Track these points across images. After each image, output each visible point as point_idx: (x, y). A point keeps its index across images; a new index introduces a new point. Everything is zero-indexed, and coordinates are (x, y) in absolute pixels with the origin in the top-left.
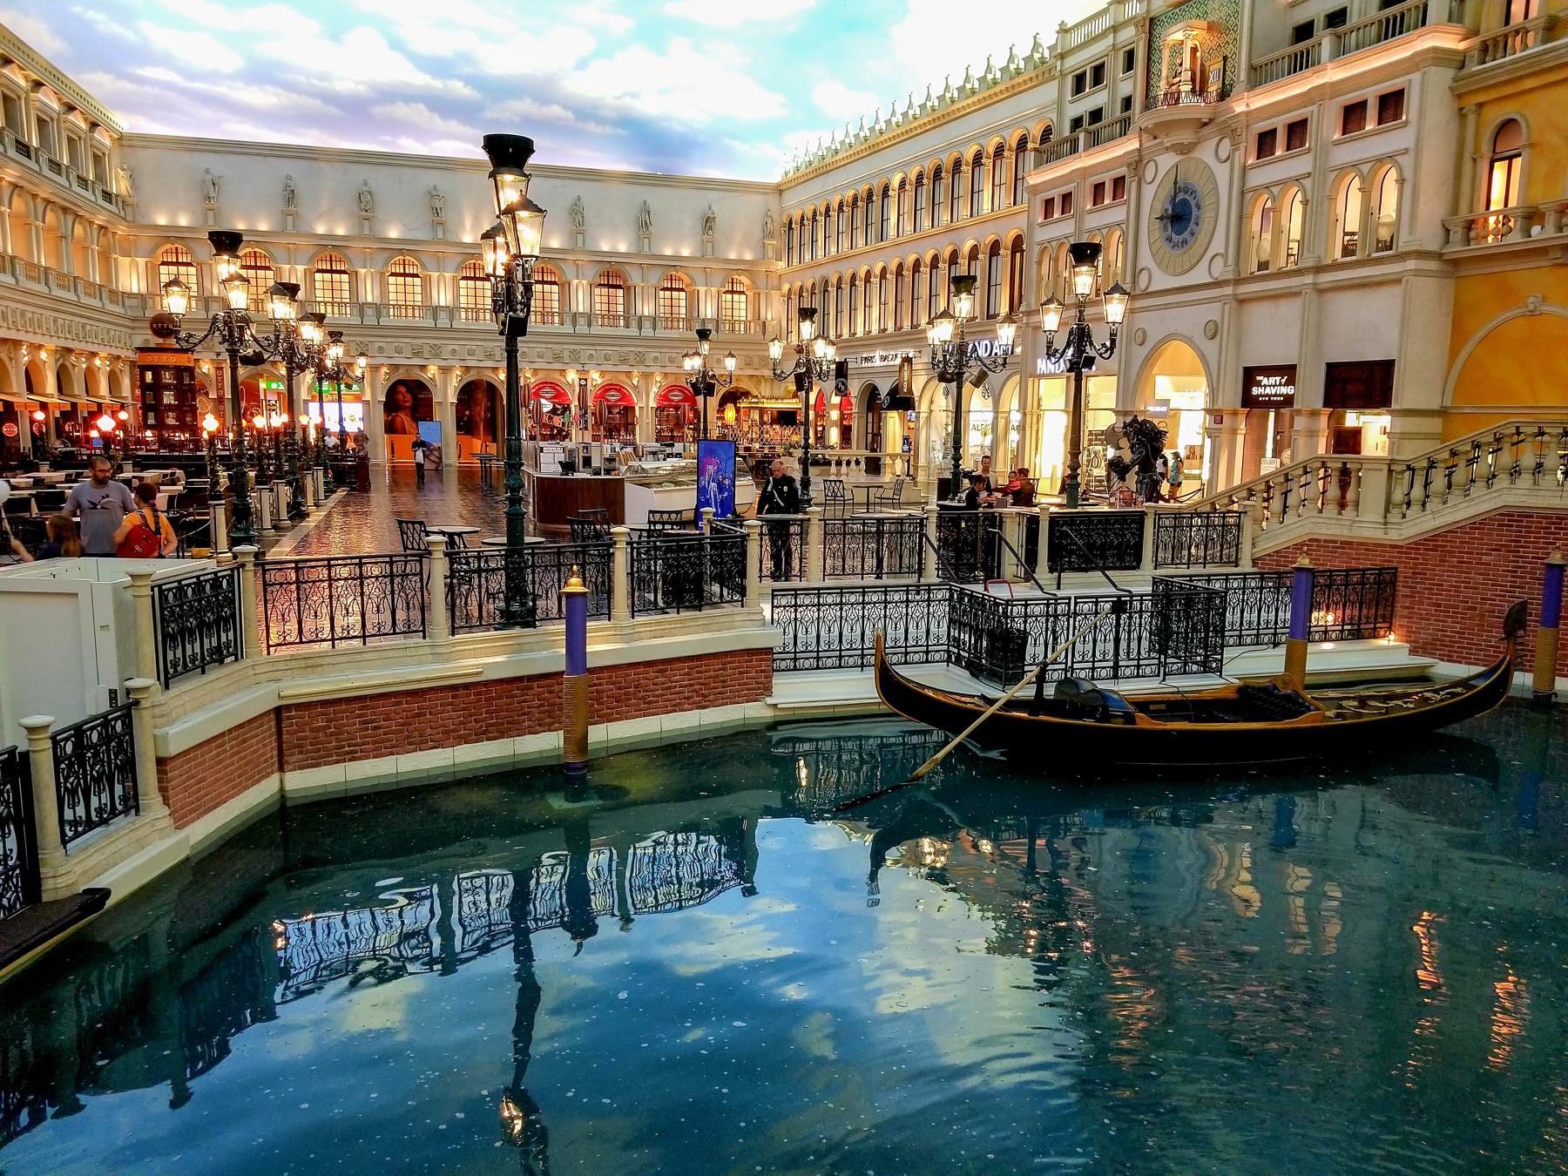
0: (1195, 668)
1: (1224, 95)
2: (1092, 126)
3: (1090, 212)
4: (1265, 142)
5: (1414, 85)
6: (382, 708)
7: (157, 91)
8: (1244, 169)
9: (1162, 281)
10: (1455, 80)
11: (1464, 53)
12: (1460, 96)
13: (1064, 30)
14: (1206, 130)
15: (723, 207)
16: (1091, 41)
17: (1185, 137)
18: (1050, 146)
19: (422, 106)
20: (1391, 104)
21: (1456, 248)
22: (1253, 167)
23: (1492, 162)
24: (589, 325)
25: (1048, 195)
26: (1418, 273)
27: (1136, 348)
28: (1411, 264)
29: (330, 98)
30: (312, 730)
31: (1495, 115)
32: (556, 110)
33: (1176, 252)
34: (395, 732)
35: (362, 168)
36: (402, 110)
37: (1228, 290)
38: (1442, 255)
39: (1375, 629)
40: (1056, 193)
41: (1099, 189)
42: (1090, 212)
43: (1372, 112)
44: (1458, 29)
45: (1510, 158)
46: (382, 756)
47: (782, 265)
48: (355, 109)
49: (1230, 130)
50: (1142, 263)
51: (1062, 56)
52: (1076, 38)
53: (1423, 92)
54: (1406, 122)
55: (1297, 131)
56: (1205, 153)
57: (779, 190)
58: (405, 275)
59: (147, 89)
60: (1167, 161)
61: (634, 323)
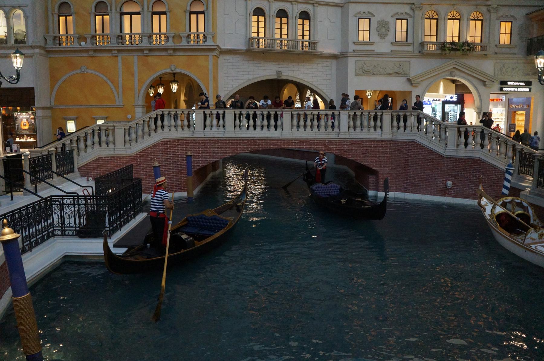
21: (50, 45)
26: (40, 54)
28: (37, 51)
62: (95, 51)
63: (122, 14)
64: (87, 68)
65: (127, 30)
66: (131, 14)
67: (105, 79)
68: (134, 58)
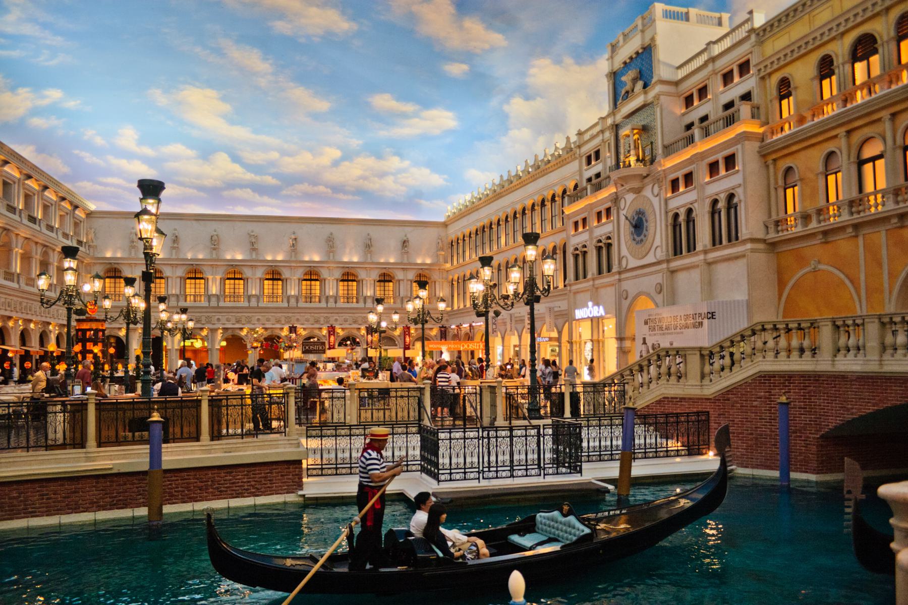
0: (564, 470)
1: (652, 161)
2: (597, 183)
3: (596, 227)
4: (675, 184)
5: (737, 149)
6: (53, 487)
7: (113, 189)
8: (666, 201)
9: (633, 263)
10: (760, 147)
11: (763, 134)
12: (764, 156)
13: (580, 134)
14: (647, 180)
15: (414, 235)
16: (593, 137)
17: (636, 184)
18: (577, 193)
19: (249, 190)
20: (730, 161)
21: (772, 236)
22: (671, 198)
23: (785, 190)
24: (336, 302)
25: (575, 219)
26: (753, 251)
27: (624, 301)
28: (749, 246)
29: (201, 188)
30: (10, 498)
31: (783, 164)
32: (321, 188)
33: (639, 246)
34: (59, 502)
35: (213, 223)
36: (238, 193)
37: (664, 266)
38: (765, 240)
39: (699, 449)
40: (579, 218)
41: (599, 214)
42: (596, 227)
43: (722, 166)
44: (756, 121)
45: (793, 187)
46: (51, 515)
47: (448, 265)
48: (215, 192)
49: (658, 181)
50: (622, 254)
51: (579, 147)
52: (587, 137)
53: (743, 154)
54: (738, 171)
55: (688, 178)
56: (647, 192)
57: (445, 225)
58: (235, 279)
59: (108, 189)
60: (630, 197)
61: (361, 300)
62: (825, 233)
63: (861, 163)
64: (819, 262)
65: (869, 187)
66: (873, 159)
67: (842, 276)
68: (881, 236)
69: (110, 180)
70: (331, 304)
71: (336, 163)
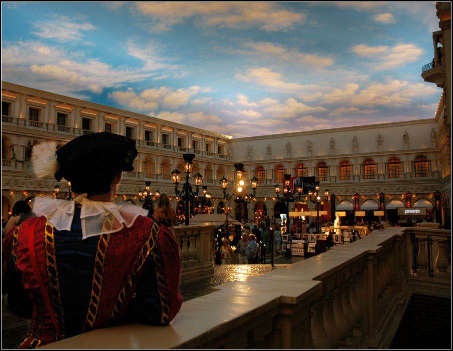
7: (243, 126)
19: (310, 116)
32: (353, 109)
36: (305, 119)
59: (241, 126)
69: (241, 122)
70: (382, 179)
71: (357, 92)
